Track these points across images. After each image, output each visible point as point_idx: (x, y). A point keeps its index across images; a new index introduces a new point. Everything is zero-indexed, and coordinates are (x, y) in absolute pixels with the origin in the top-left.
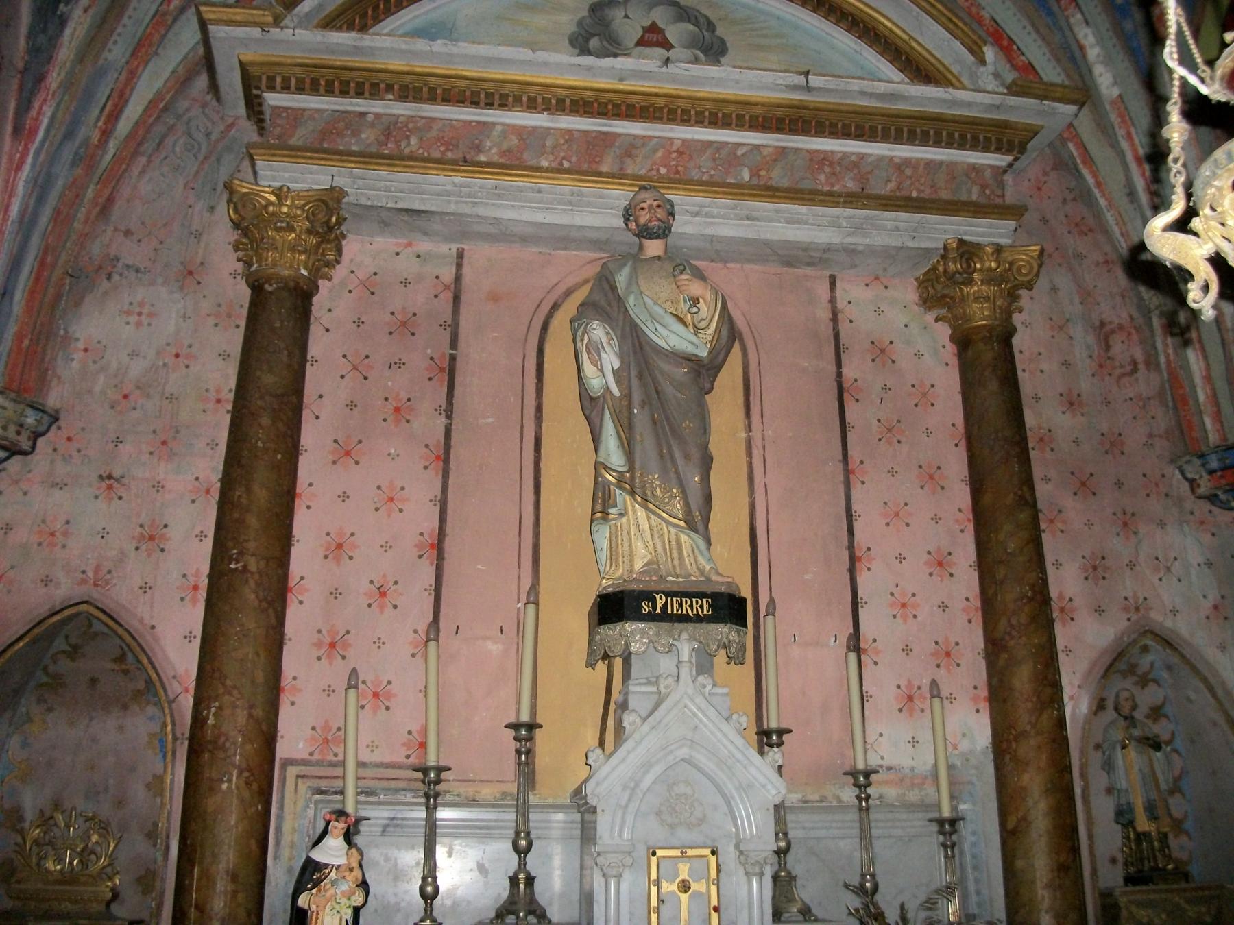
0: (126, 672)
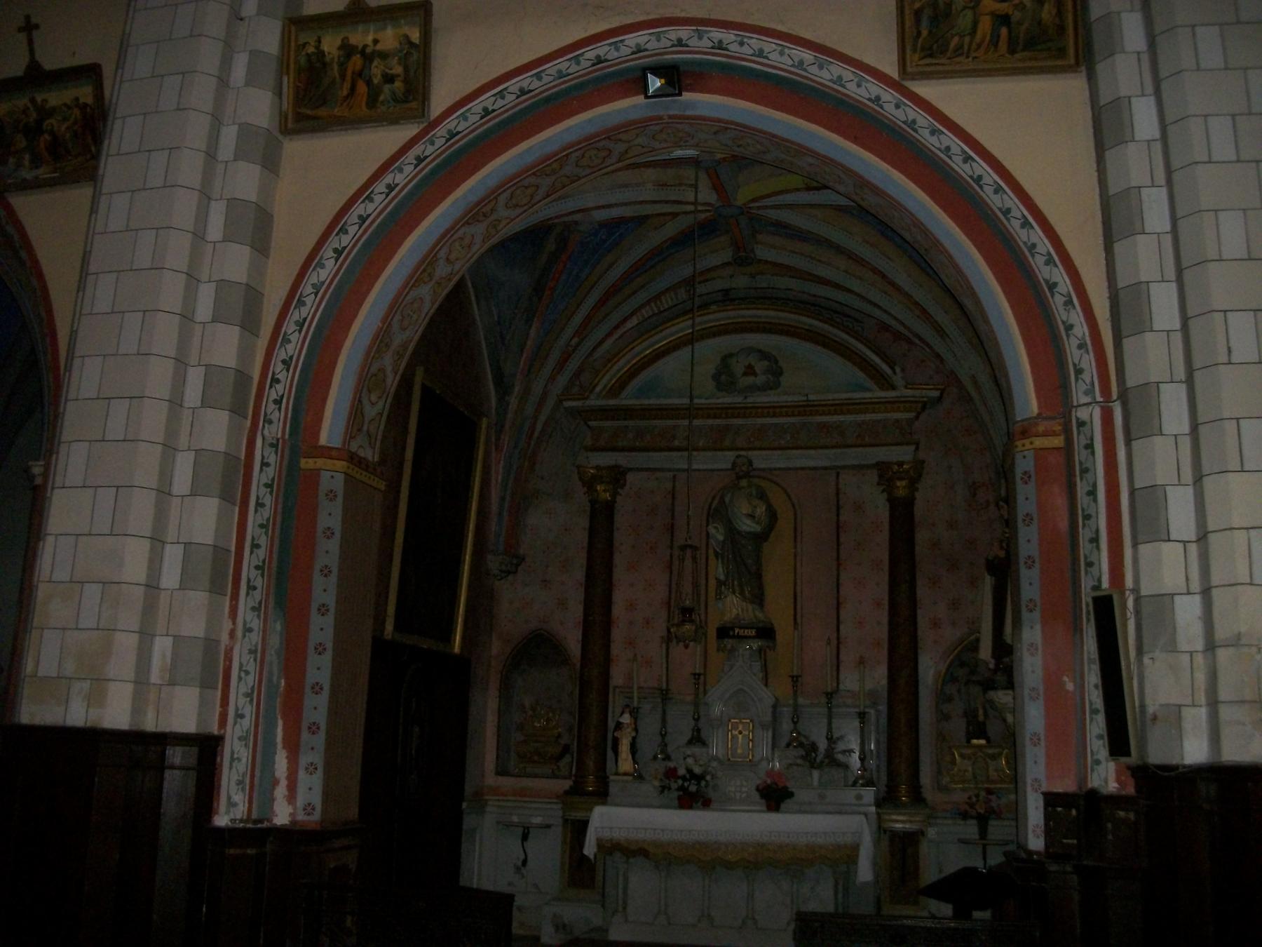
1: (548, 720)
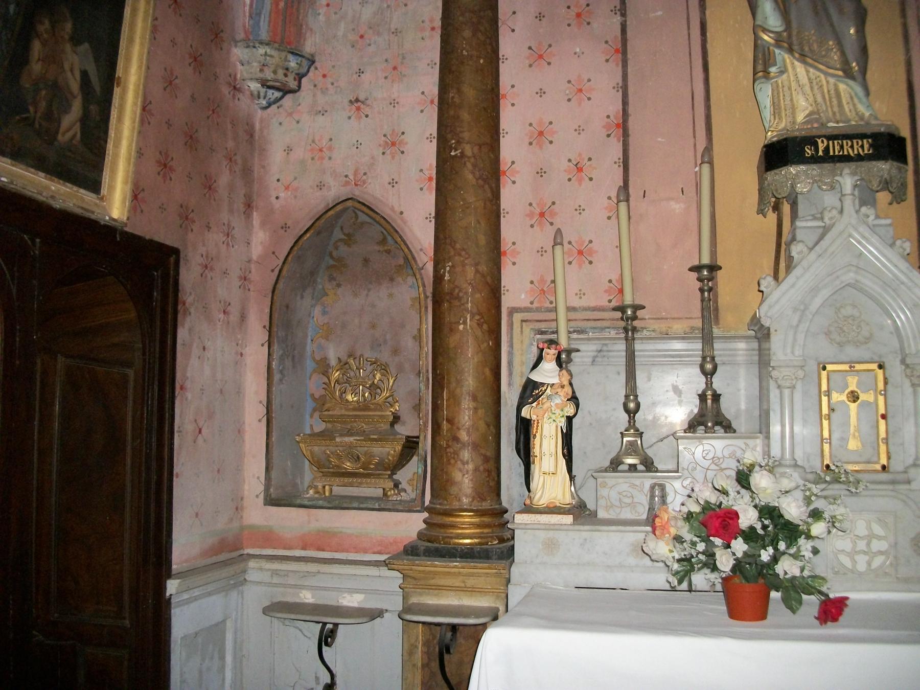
0: (388, 252)
1: (374, 388)
